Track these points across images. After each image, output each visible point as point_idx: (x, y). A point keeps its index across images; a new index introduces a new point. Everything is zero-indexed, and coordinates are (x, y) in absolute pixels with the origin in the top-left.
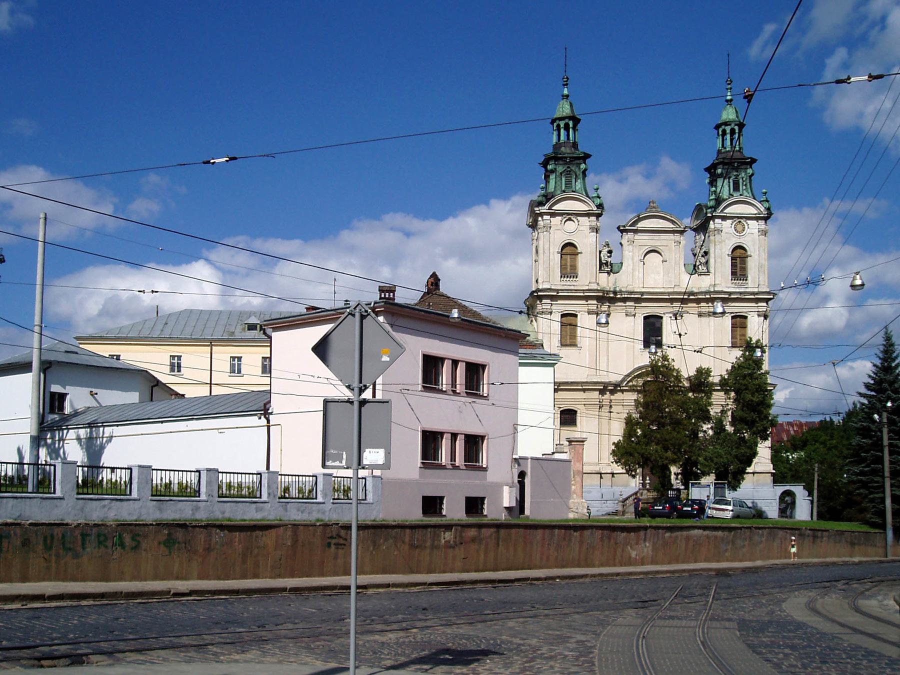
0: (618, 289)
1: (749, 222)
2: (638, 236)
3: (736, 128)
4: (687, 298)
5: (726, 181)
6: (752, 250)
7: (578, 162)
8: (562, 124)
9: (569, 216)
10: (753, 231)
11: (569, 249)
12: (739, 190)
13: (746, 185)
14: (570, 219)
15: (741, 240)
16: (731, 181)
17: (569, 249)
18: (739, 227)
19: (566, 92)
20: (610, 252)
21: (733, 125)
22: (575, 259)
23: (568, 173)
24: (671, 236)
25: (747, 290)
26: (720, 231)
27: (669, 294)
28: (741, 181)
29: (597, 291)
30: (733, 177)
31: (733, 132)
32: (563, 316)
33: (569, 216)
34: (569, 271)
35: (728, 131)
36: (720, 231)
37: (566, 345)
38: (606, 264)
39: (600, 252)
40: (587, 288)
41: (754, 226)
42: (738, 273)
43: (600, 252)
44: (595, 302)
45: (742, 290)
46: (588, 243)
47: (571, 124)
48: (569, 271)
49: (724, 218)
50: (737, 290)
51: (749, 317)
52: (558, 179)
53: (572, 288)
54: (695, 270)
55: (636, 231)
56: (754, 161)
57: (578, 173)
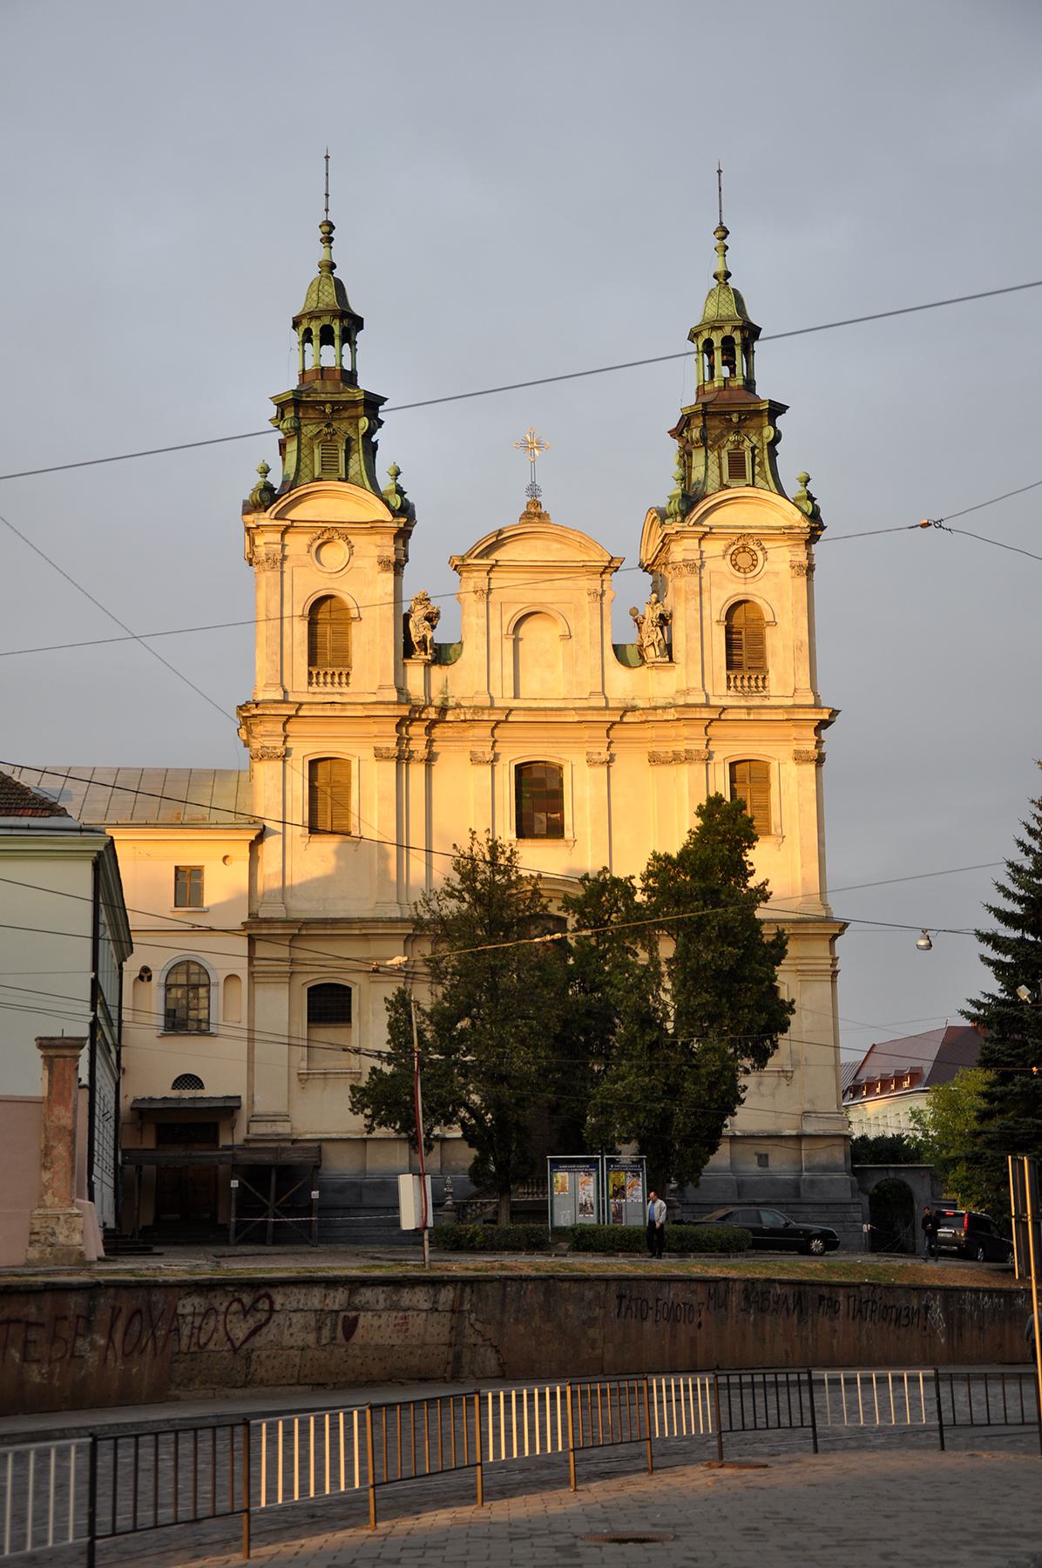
0: (451, 703)
3: (737, 336)
4: (617, 720)
5: (713, 456)
9: (326, 534)
12: (744, 477)
13: (761, 464)
15: (750, 588)
16: (724, 455)
18: (744, 559)
20: (432, 619)
22: (345, 634)
23: (327, 442)
25: (767, 703)
28: (748, 455)
30: (729, 446)
35: (717, 343)
38: (423, 642)
39: (407, 617)
40: (374, 699)
45: (756, 702)
46: (368, 592)
50: (743, 703)
51: (774, 766)
53: (337, 698)
56: (777, 409)
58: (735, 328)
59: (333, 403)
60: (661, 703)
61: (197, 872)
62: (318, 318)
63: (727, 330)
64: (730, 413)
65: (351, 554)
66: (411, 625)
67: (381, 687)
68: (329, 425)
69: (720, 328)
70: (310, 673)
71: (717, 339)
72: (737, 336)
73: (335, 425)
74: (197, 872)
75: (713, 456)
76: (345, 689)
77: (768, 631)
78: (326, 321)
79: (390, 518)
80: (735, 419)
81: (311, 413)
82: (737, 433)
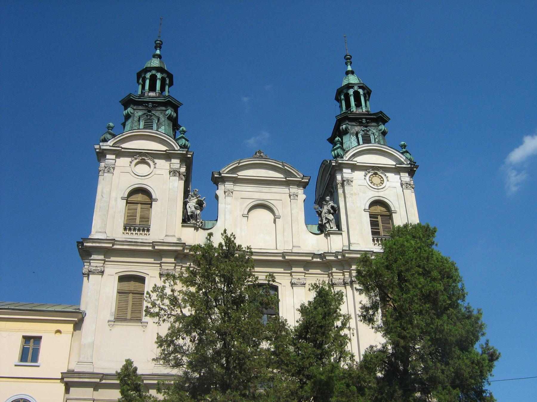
1: (388, 174)
2: (239, 187)
3: (361, 91)
6: (397, 205)
7: (164, 108)
8: (148, 75)
10: (394, 185)
11: (140, 197)
14: (143, 162)
15: (380, 194)
17: (140, 197)
19: (158, 52)
21: (356, 88)
24: (284, 190)
26: (349, 181)
27: (283, 254)
28: (372, 137)
29: (176, 244)
30: (362, 133)
31: (356, 94)
32: (122, 279)
33: (143, 157)
34: (137, 223)
36: (349, 181)
37: (125, 320)
41: (393, 180)
42: (382, 233)
43: (185, 204)
44: (172, 260)
47: (159, 75)
48: (137, 223)
49: (354, 168)
52: (136, 124)
54: (322, 229)
55: (236, 181)
57: (162, 119)
58: (360, 87)
59: (153, 103)
60: (334, 251)
61: (38, 339)
62: (150, 71)
63: (356, 88)
64: (362, 118)
65: (155, 168)
66: (188, 206)
67: (166, 236)
68: (150, 111)
69: (352, 87)
70: (125, 229)
71: (351, 92)
72: (361, 91)
73: (153, 112)
74: (38, 339)
75: (354, 138)
76: (145, 237)
77: (394, 215)
78: (154, 72)
79: (177, 148)
80: (364, 121)
81: (140, 107)
82: (366, 127)
